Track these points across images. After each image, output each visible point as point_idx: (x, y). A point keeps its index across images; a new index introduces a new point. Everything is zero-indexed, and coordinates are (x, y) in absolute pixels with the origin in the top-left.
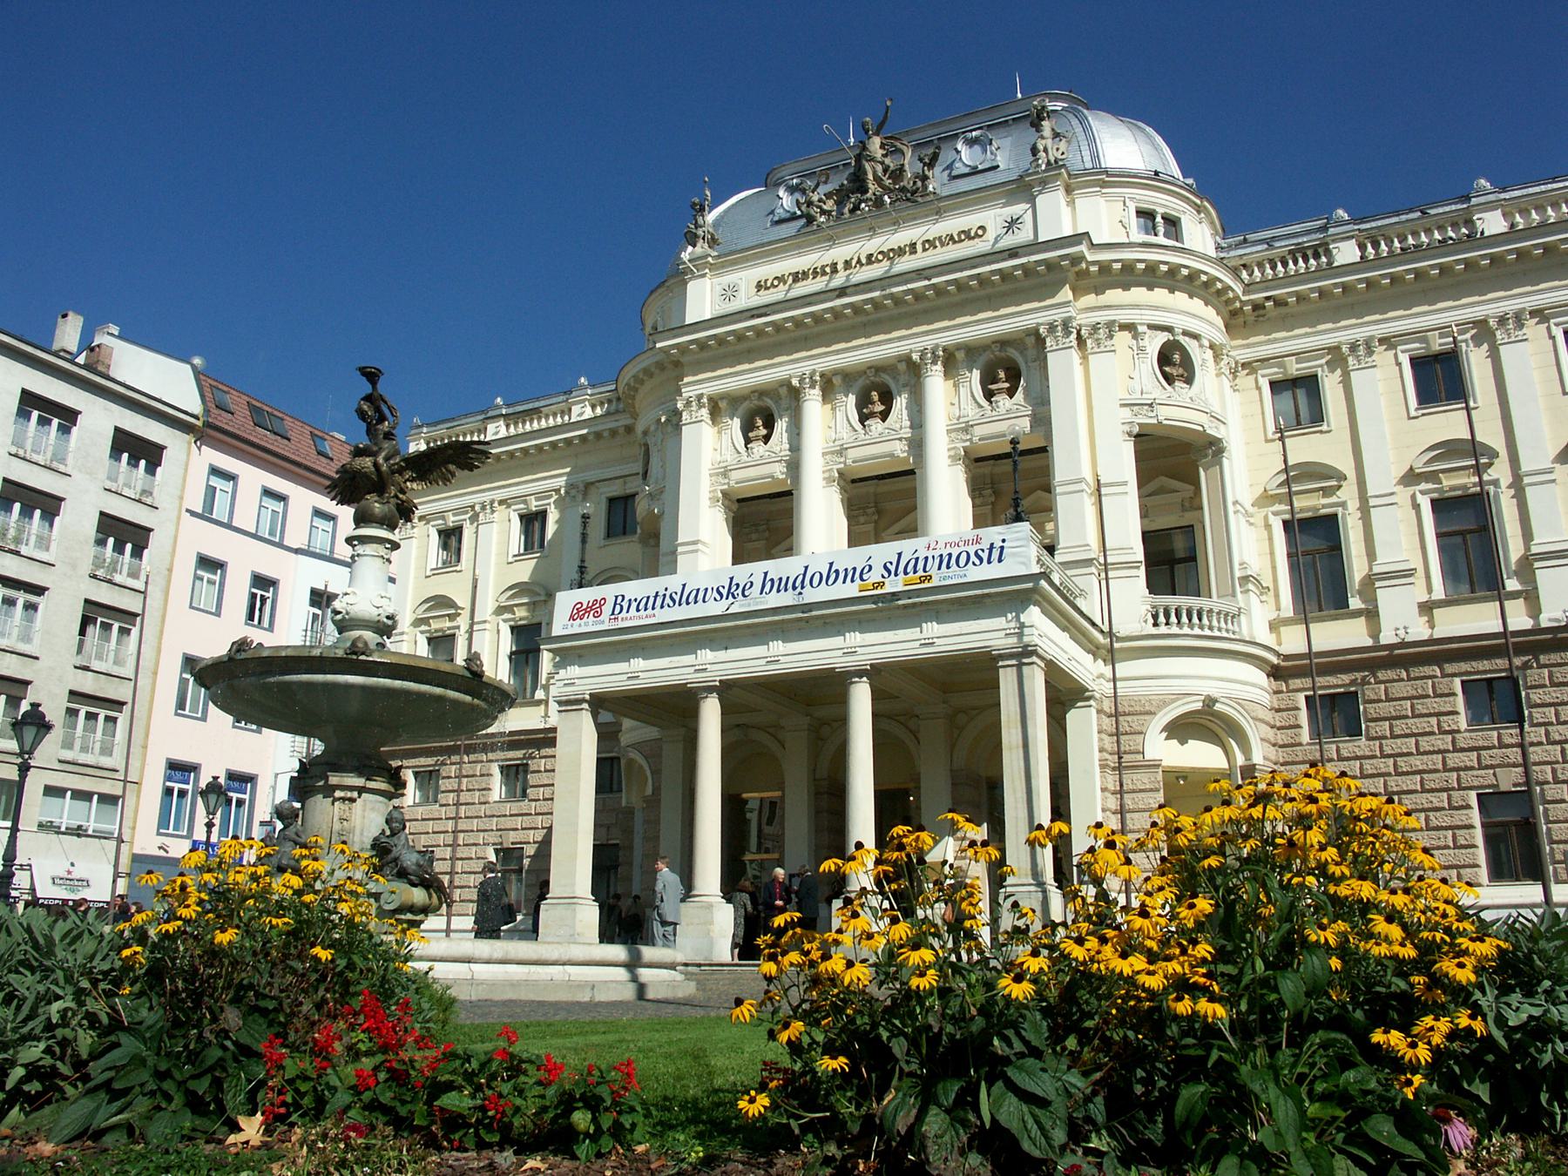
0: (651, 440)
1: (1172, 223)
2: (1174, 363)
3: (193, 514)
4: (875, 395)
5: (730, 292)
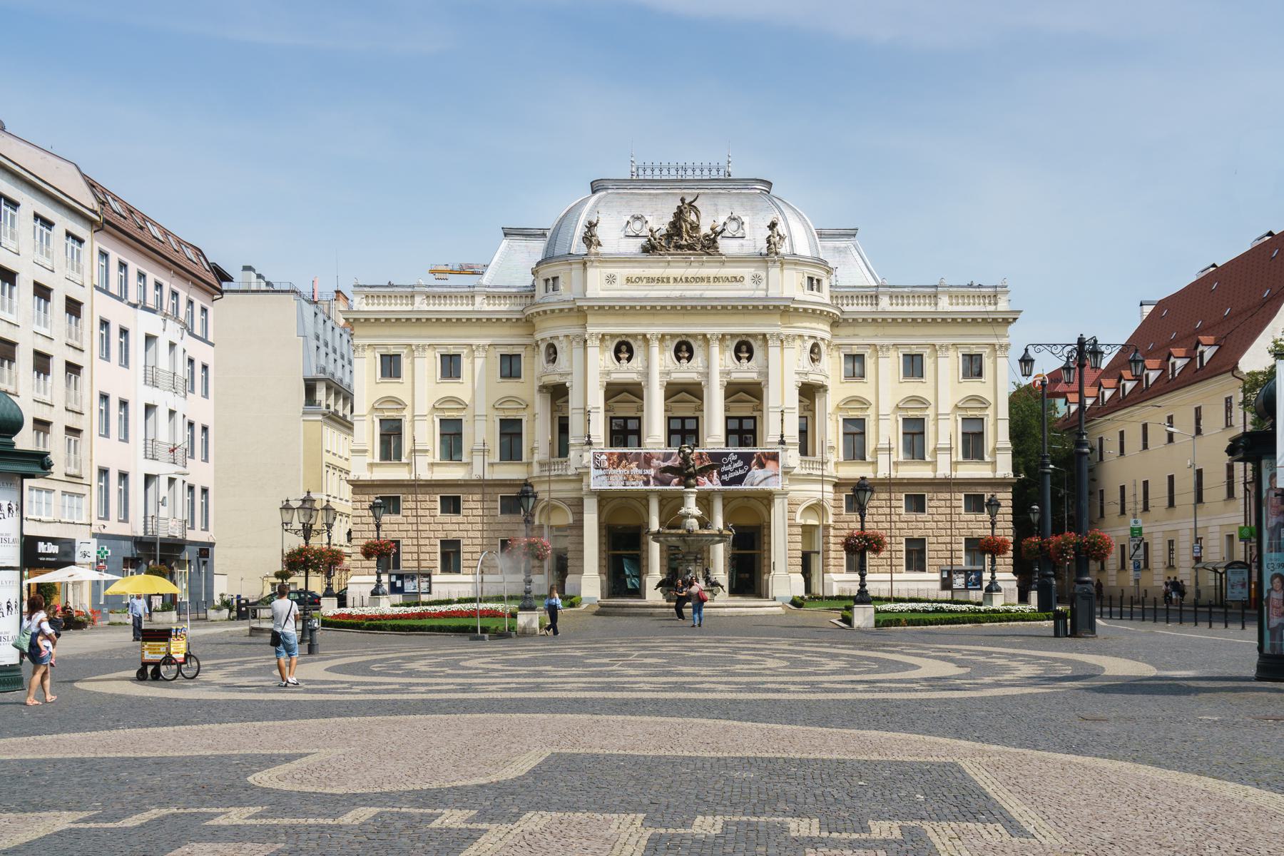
0: (556, 343)
1: (818, 281)
2: (815, 352)
3: (97, 288)
4: (684, 348)
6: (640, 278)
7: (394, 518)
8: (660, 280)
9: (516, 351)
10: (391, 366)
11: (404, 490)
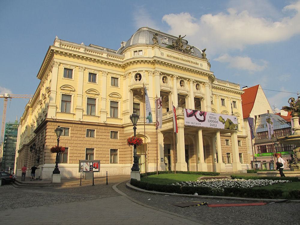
0: (140, 73)
5: (162, 54)
6: (171, 56)
7: (66, 137)
8: (177, 58)
9: (117, 77)
10: (68, 73)
11: (71, 125)
